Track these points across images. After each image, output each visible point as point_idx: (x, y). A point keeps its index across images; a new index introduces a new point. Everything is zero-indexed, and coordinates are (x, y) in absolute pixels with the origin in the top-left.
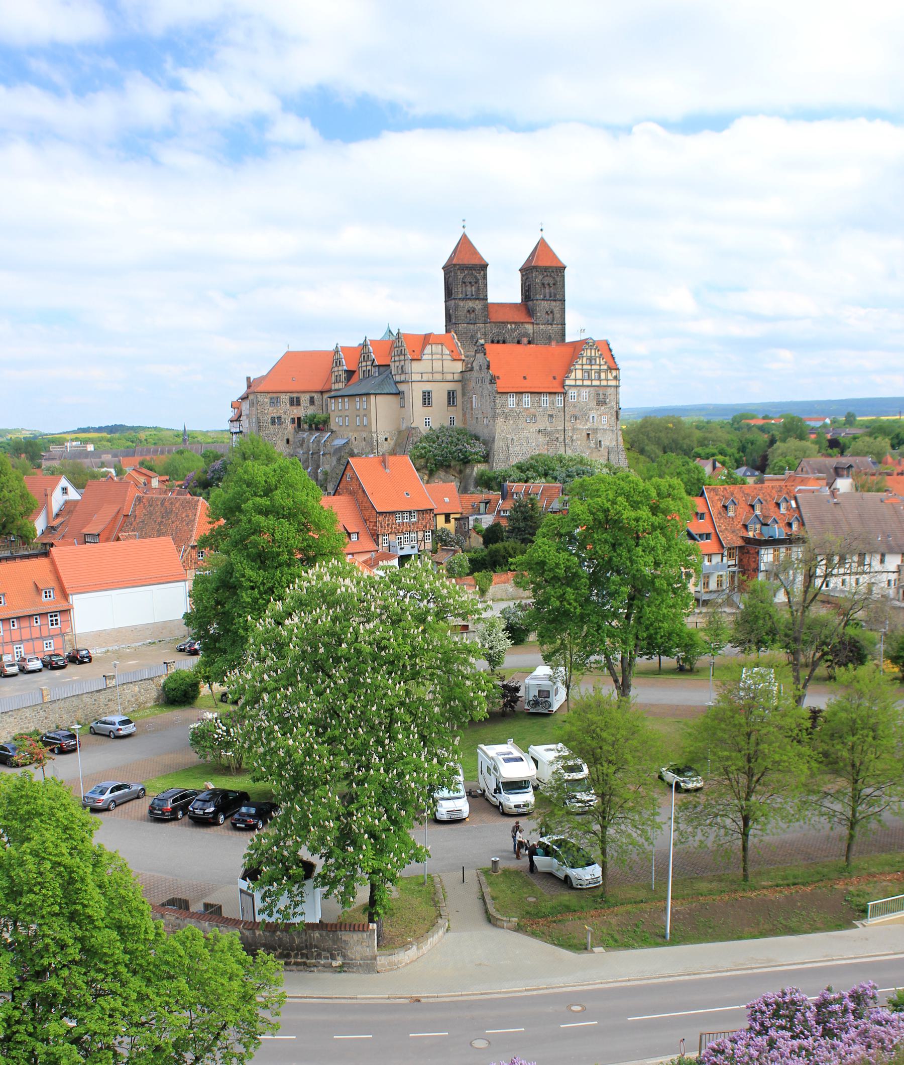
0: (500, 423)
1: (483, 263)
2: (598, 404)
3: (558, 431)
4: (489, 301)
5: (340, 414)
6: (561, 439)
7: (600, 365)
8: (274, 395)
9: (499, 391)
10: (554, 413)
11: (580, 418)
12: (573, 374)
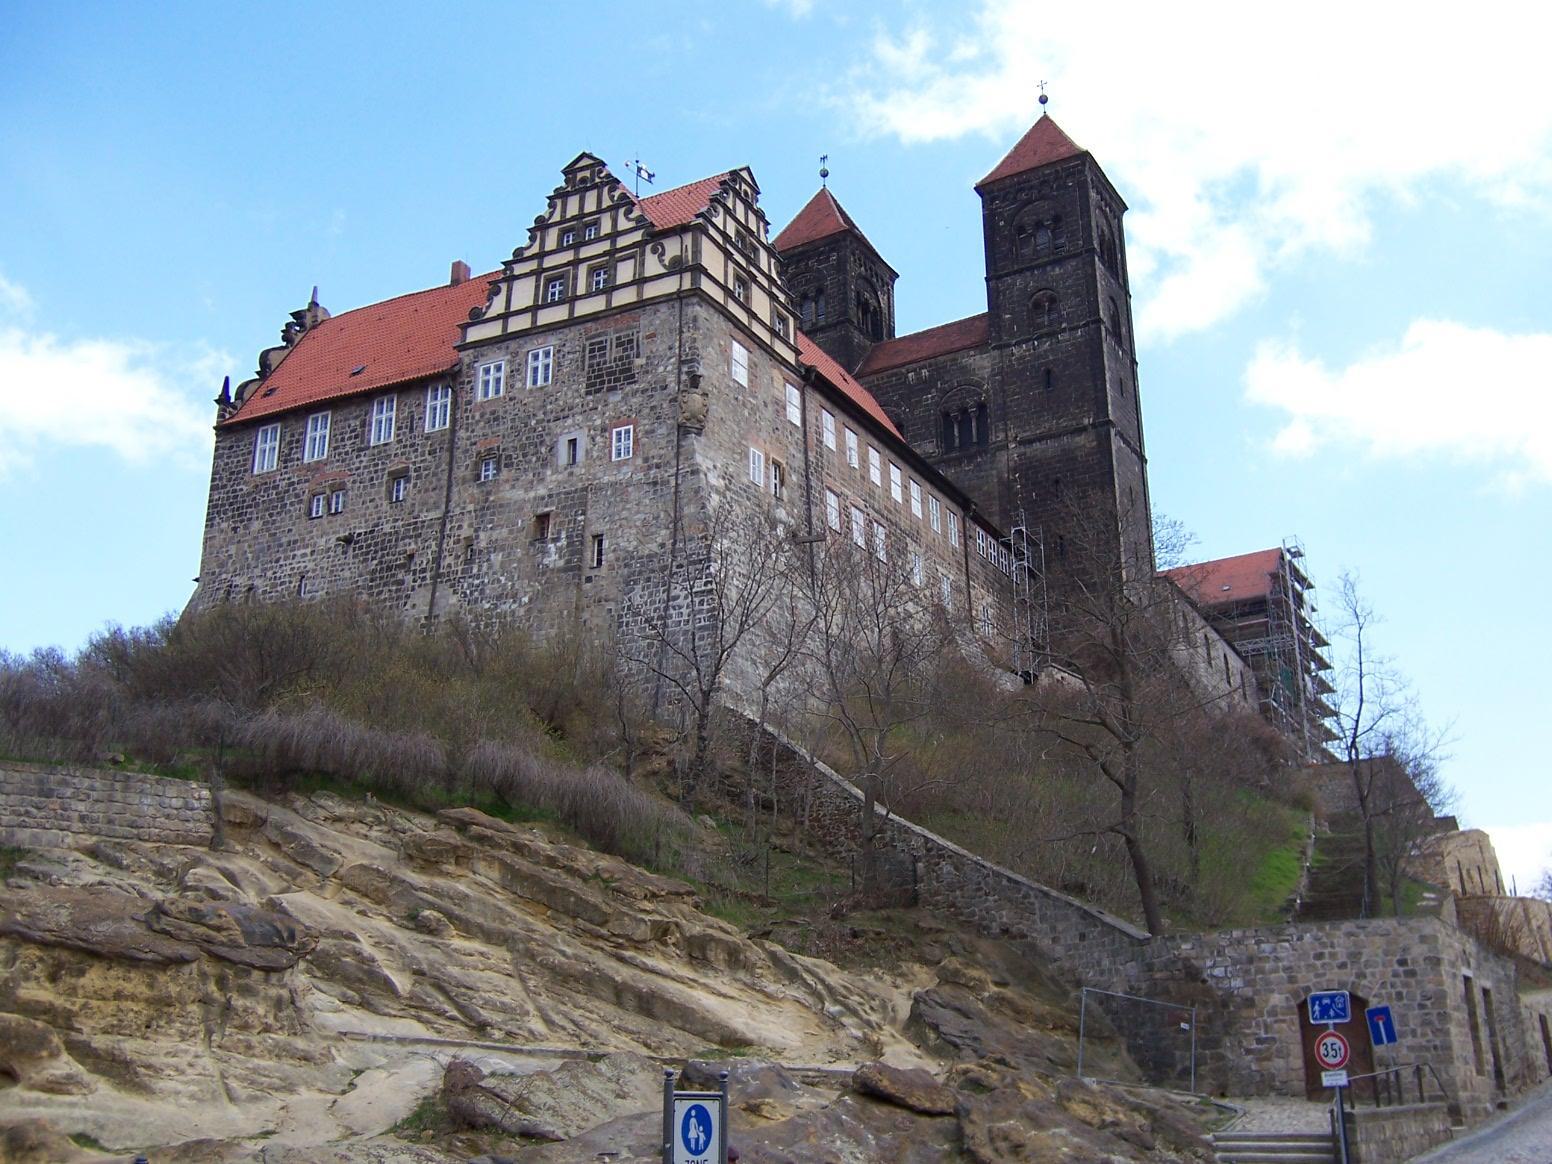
2: (593, 388)
3: (416, 529)
6: (423, 560)
11: (517, 456)
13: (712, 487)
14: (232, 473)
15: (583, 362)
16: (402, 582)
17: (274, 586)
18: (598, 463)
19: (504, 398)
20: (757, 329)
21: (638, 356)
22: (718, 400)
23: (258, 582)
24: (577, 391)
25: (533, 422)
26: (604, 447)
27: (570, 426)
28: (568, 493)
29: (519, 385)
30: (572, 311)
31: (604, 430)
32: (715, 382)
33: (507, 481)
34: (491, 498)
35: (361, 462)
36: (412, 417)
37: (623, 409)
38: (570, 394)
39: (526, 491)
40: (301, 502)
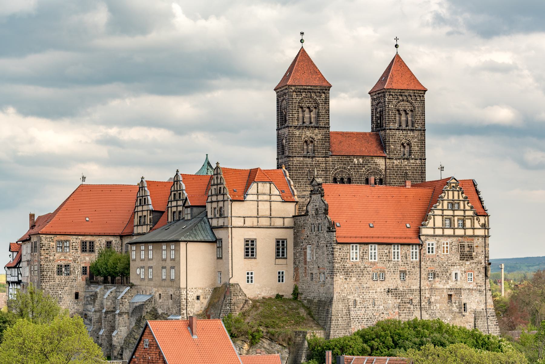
0: (340, 281)
1: (324, 84)
3: (411, 291)
4: (331, 130)
5: (142, 264)
6: (416, 301)
7: (464, 211)
8: (63, 238)
9: (339, 240)
10: (407, 268)
11: (440, 275)
12: (431, 221)
14: (342, 259)
15: (458, 249)
16: (410, 308)
17: (363, 301)
18: (464, 282)
23: (357, 299)
24: (457, 258)
25: (445, 265)
26: (465, 277)
28: (456, 289)
29: (440, 252)
31: (465, 272)
34: (433, 286)
35: (390, 265)
36: (406, 254)
37: (470, 267)
38: (455, 259)
40: (369, 274)
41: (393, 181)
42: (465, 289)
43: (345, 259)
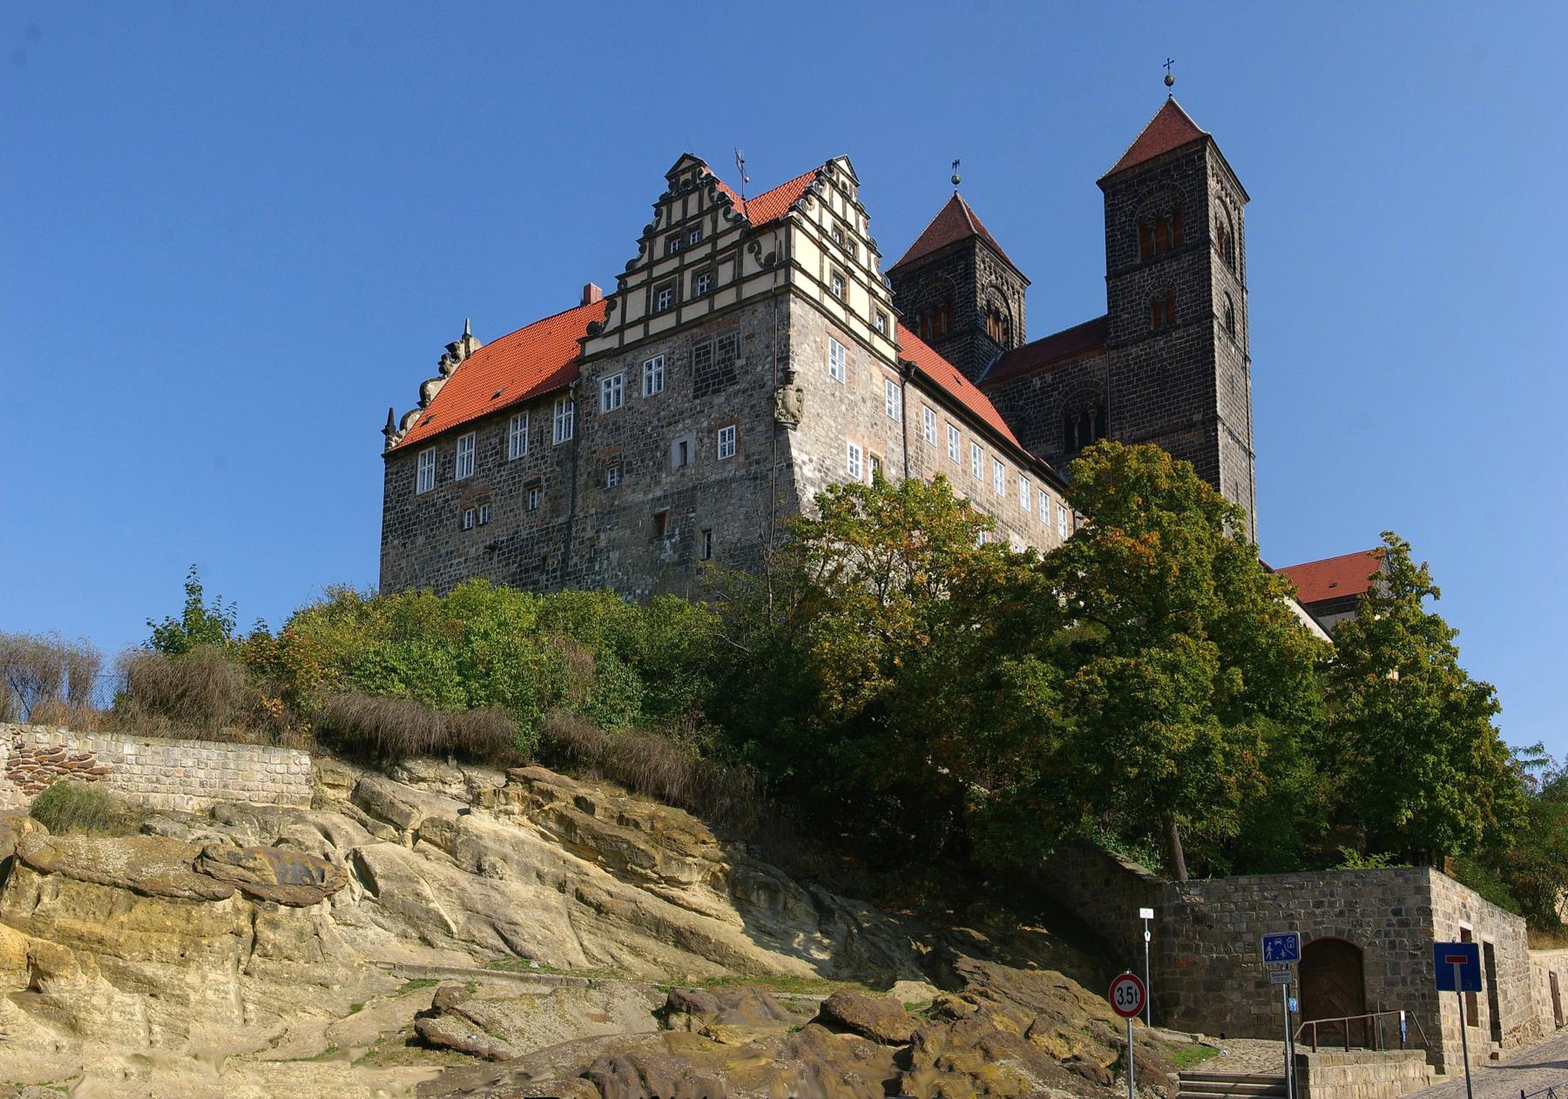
2: (699, 392)
13: (807, 479)
15: (691, 366)
18: (706, 463)
19: (624, 408)
20: (855, 325)
21: (739, 358)
22: (814, 395)
26: (710, 448)
27: (680, 431)
28: (680, 493)
29: (635, 395)
30: (679, 318)
31: (710, 431)
32: (811, 379)
33: (628, 486)
35: (502, 476)
37: (726, 410)
38: (680, 399)
39: (645, 494)
40: (454, 516)
41: (1127, 401)
42: (709, 487)
43: (405, 494)
